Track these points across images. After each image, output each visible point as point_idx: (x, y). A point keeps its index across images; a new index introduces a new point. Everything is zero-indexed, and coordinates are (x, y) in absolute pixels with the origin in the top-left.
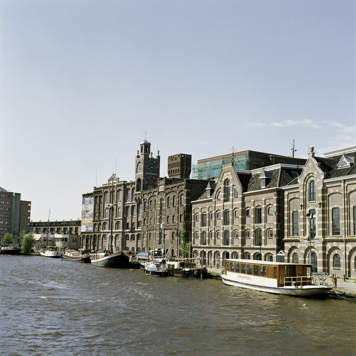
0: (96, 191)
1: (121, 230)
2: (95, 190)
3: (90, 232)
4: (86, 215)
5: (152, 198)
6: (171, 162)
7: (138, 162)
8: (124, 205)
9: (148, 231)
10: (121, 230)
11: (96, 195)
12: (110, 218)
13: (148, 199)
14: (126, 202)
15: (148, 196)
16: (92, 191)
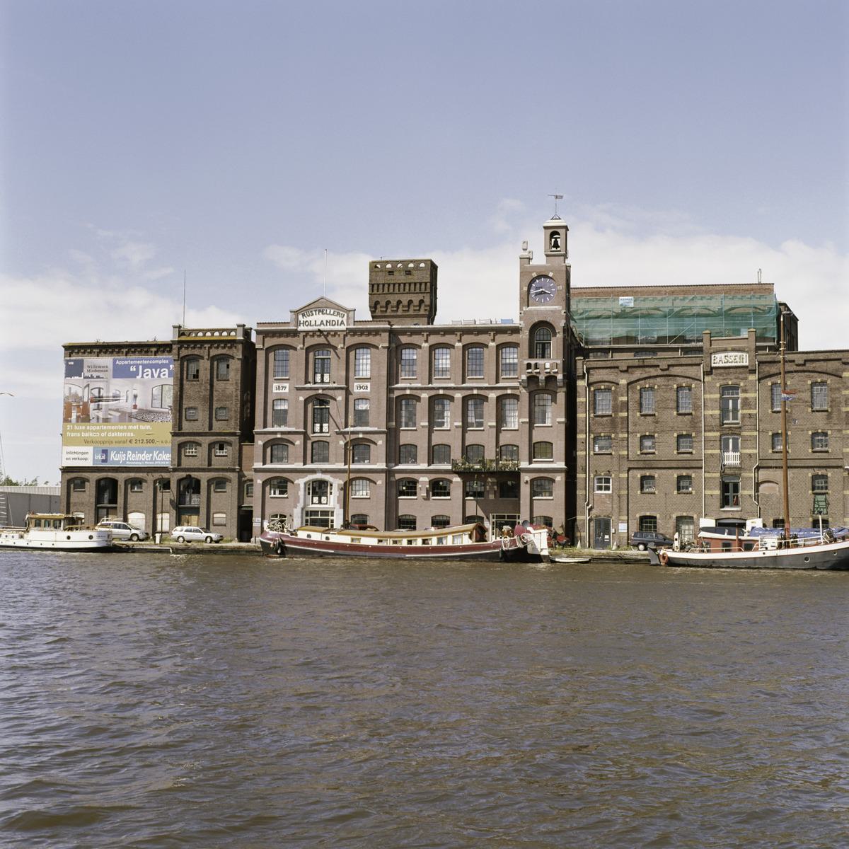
0: (183, 338)
1: (382, 466)
2: (182, 334)
3: (165, 469)
4: (93, 414)
5: (652, 381)
6: (381, 279)
7: (534, 275)
8: (390, 391)
9: (628, 471)
10: (382, 466)
11: (184, 352)
12: (305, 427)
13: (623, 382)
14: (397, 383)
15: (625, 375)
16: (167, 336)
